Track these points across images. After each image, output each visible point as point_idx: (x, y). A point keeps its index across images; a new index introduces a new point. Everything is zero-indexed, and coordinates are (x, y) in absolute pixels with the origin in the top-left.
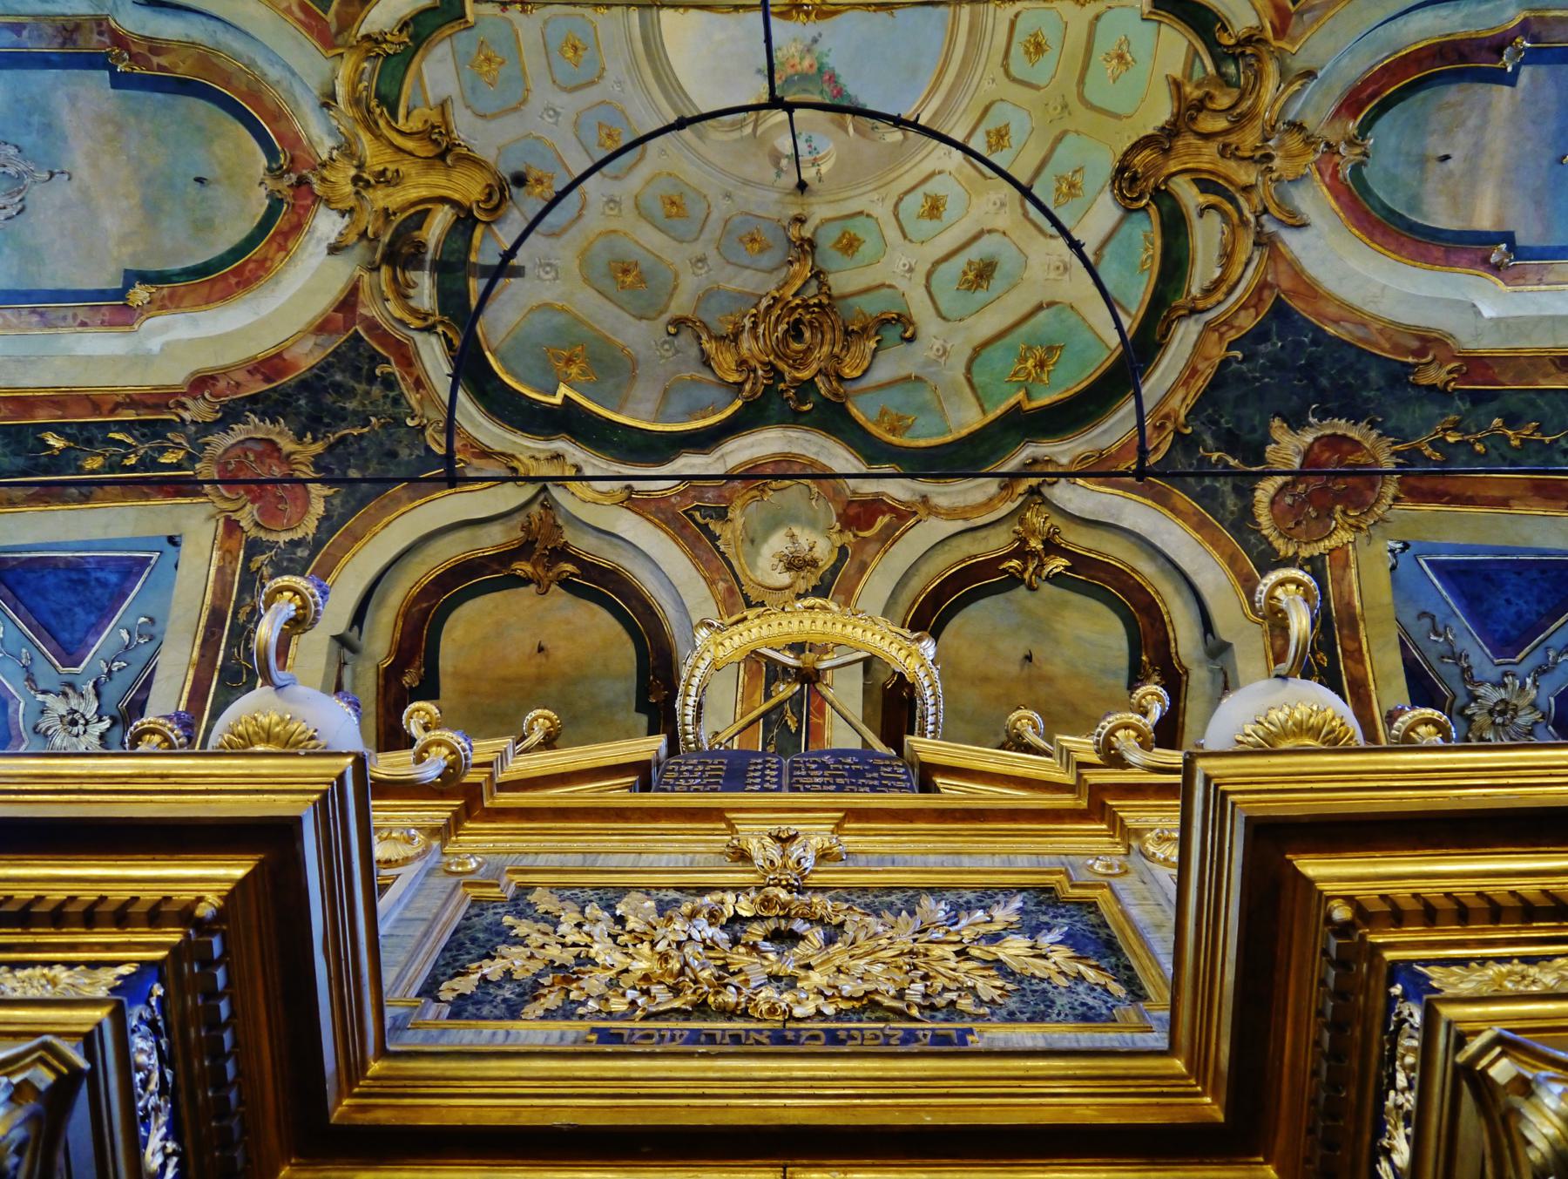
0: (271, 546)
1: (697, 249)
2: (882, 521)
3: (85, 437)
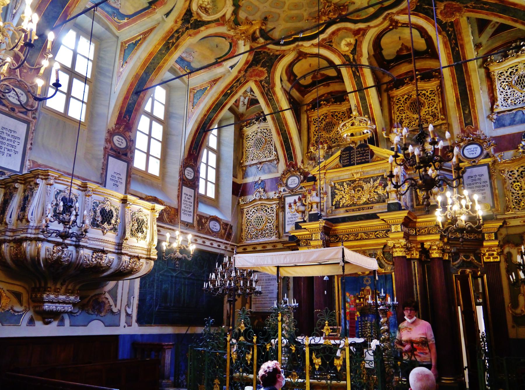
0: (263, 80)
1: (304, 9)
2: (361, 32)
3: (232, 88)
